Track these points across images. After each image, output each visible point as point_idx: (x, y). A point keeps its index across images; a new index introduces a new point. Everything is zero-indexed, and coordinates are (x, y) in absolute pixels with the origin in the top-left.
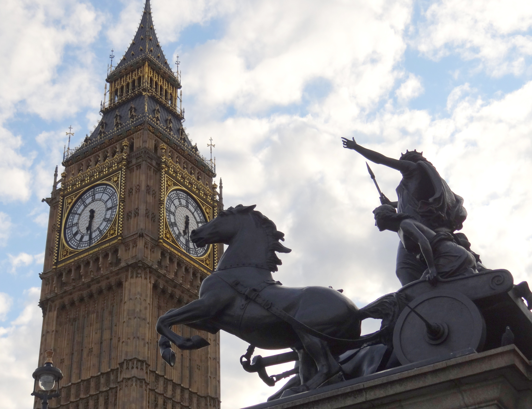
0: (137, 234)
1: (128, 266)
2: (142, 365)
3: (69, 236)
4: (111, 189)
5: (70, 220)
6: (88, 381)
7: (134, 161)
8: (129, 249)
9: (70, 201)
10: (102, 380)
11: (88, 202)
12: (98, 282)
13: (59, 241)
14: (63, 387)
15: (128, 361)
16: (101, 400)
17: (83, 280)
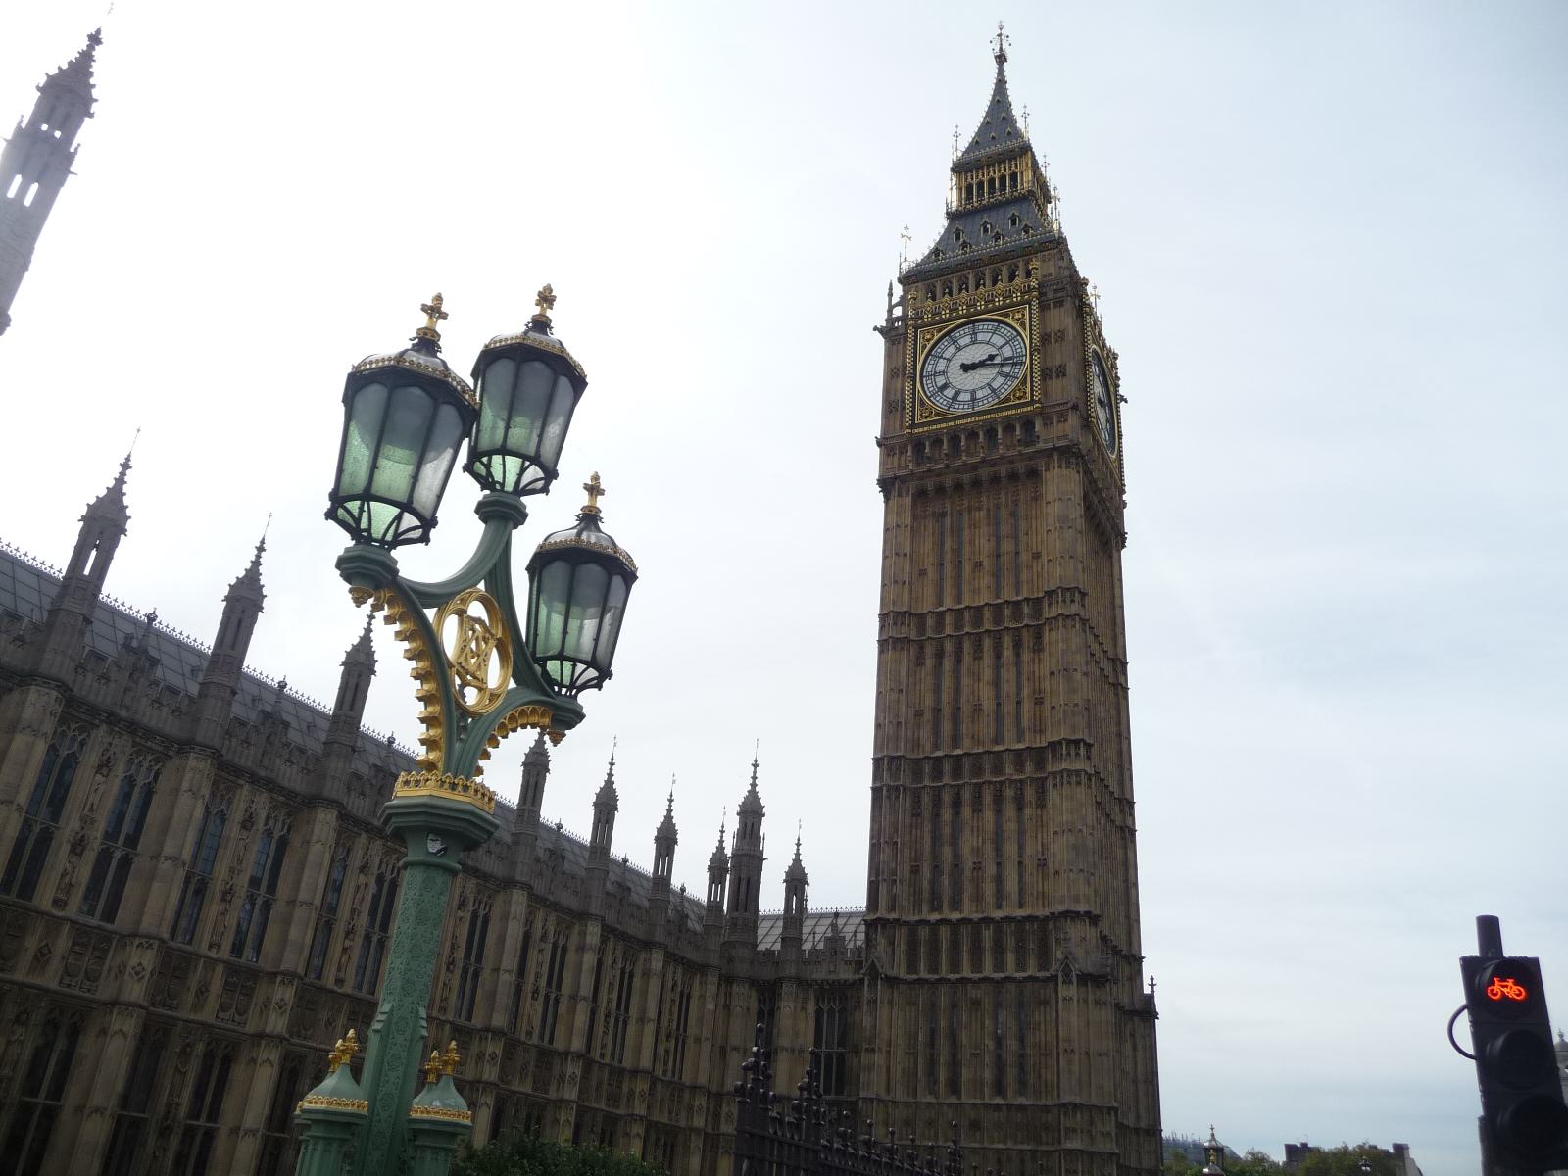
0: (1067, 403)
1: (1055, 448)
2: (1083, 599)
3: (930, 389)
4: (1009, 329)
5: (930, 366)
6: (979, 609)
7: (1050, 295)
8: (1052, 423)
10: (1007, 612)
11: (962, 342)
12: (994, 465)
13: (914, 394)
14: (930, 612)
16: (1007, 641)
17: (964, 458)
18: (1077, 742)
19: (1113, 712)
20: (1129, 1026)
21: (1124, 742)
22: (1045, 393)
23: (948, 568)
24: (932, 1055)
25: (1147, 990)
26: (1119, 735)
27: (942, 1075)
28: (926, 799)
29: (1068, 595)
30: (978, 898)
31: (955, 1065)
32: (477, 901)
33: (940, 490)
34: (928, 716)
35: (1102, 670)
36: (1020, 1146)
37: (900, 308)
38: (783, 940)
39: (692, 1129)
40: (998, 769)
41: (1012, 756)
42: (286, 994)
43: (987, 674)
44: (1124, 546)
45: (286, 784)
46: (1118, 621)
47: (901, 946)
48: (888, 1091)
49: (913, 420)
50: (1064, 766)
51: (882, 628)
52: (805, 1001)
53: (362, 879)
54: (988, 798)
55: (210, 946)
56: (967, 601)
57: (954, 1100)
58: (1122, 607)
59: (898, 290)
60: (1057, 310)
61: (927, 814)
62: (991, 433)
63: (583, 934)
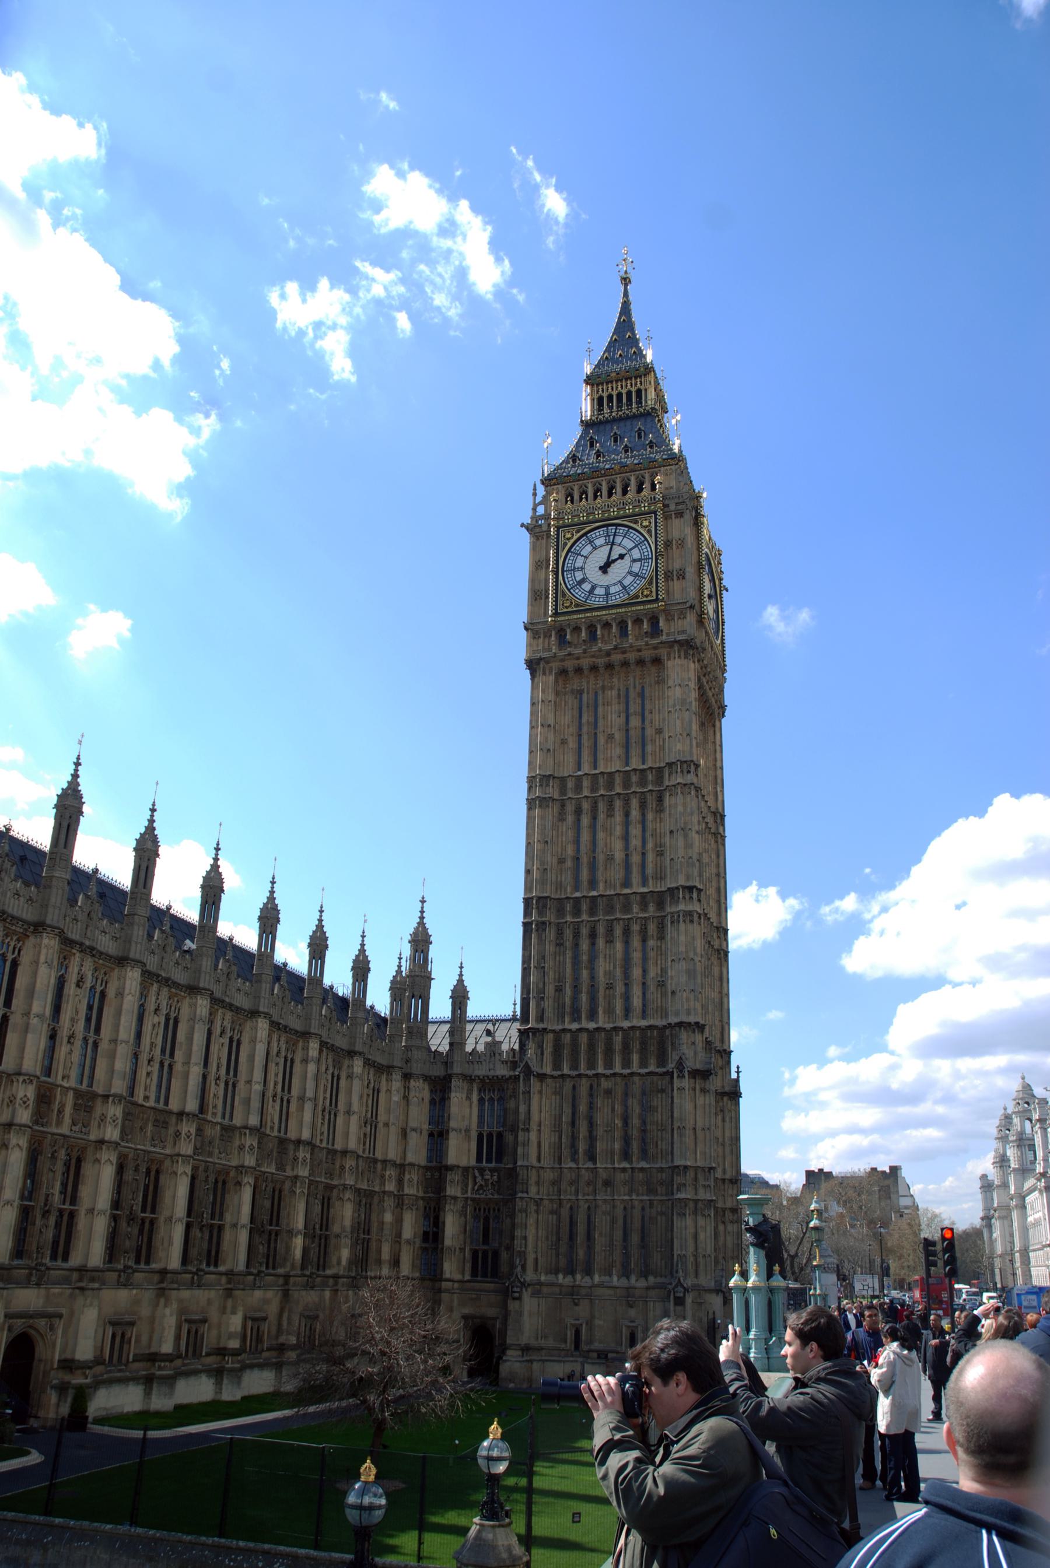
1: (675, 641)
3: (570, 583)
6: (611, 775)
7: (672, 507)
9: (568, 535)
10: (634, 778)
12: (624, 653)
13: (557, 586)
15: (682, 762)
16: (635, 803)
18: (690, 889)
19: (714, 856)
20: (721, 1104)
21: (722, 881)
22: (668, 592)
23: (585, 737)
24: (573, 1132)
25: (734, 1076)
26: (718, 875)
27: (582, 1147)
28: (568, 933)
29: (685, 766)
30: (610, 1011)
31: (592, 1139)
32: (233, 1029)
33: (579, 670)
34: (569, 863)
35: (707, 823)
36: (641, 1198)
37: (543, 507)
38: (451, 1044)
39: (384, 1192)
40: (627, 908)
41: (638, 897)
42: (115, 1111)
43: (618, 830)
44: (723, 716)
45: (102, 949)
46: (719, 781)
47: (548, 1049)
48: (539, 1161)
49: (556, 609)
50: (682, 907)
51: (530, 788)
52: (470, 1092)
53: (156, 1019)
54: (618, 931)
55: (63, 1078)
56: (601, 769)
57: (590, 1165)
58: (722, 768)
59: (541, 491)
60: (677, 520)
61: (568, 944)
62: (623, 626)
63: (306, 1049)
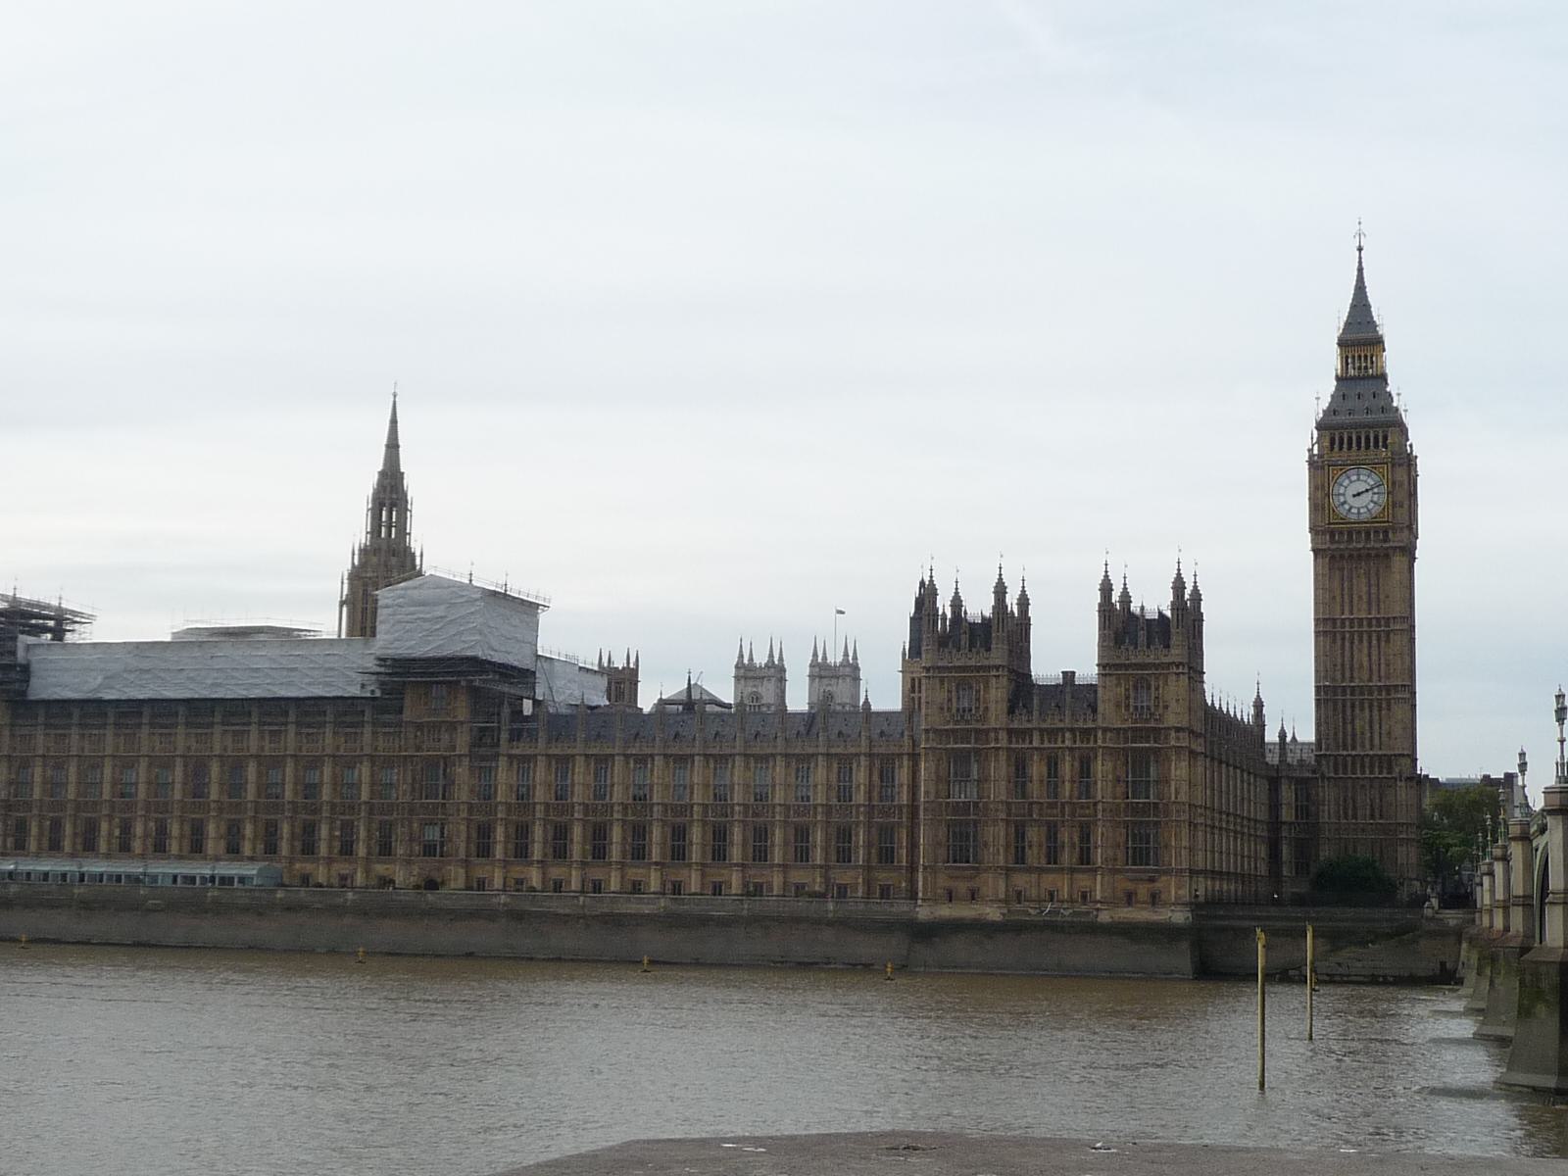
3: (1337, 503)
10: (1374, 622)
16: (1374, 638)
23: (1346, 597)
27: (1350, 812)
28: (1340, 704)
30: (1363, 746)
31: (1355, 808)
33: (1342, 557)
34: (1339, 667)
43: (1366, 651)
47: (1331, 764)
54: (1366, 705)
59: (1315, 433)
61: (1340, 710)
62: (1368, 534)
